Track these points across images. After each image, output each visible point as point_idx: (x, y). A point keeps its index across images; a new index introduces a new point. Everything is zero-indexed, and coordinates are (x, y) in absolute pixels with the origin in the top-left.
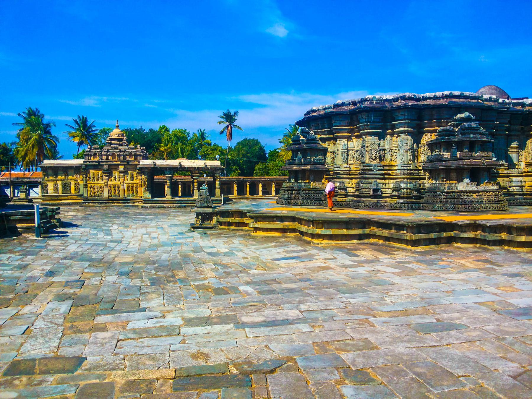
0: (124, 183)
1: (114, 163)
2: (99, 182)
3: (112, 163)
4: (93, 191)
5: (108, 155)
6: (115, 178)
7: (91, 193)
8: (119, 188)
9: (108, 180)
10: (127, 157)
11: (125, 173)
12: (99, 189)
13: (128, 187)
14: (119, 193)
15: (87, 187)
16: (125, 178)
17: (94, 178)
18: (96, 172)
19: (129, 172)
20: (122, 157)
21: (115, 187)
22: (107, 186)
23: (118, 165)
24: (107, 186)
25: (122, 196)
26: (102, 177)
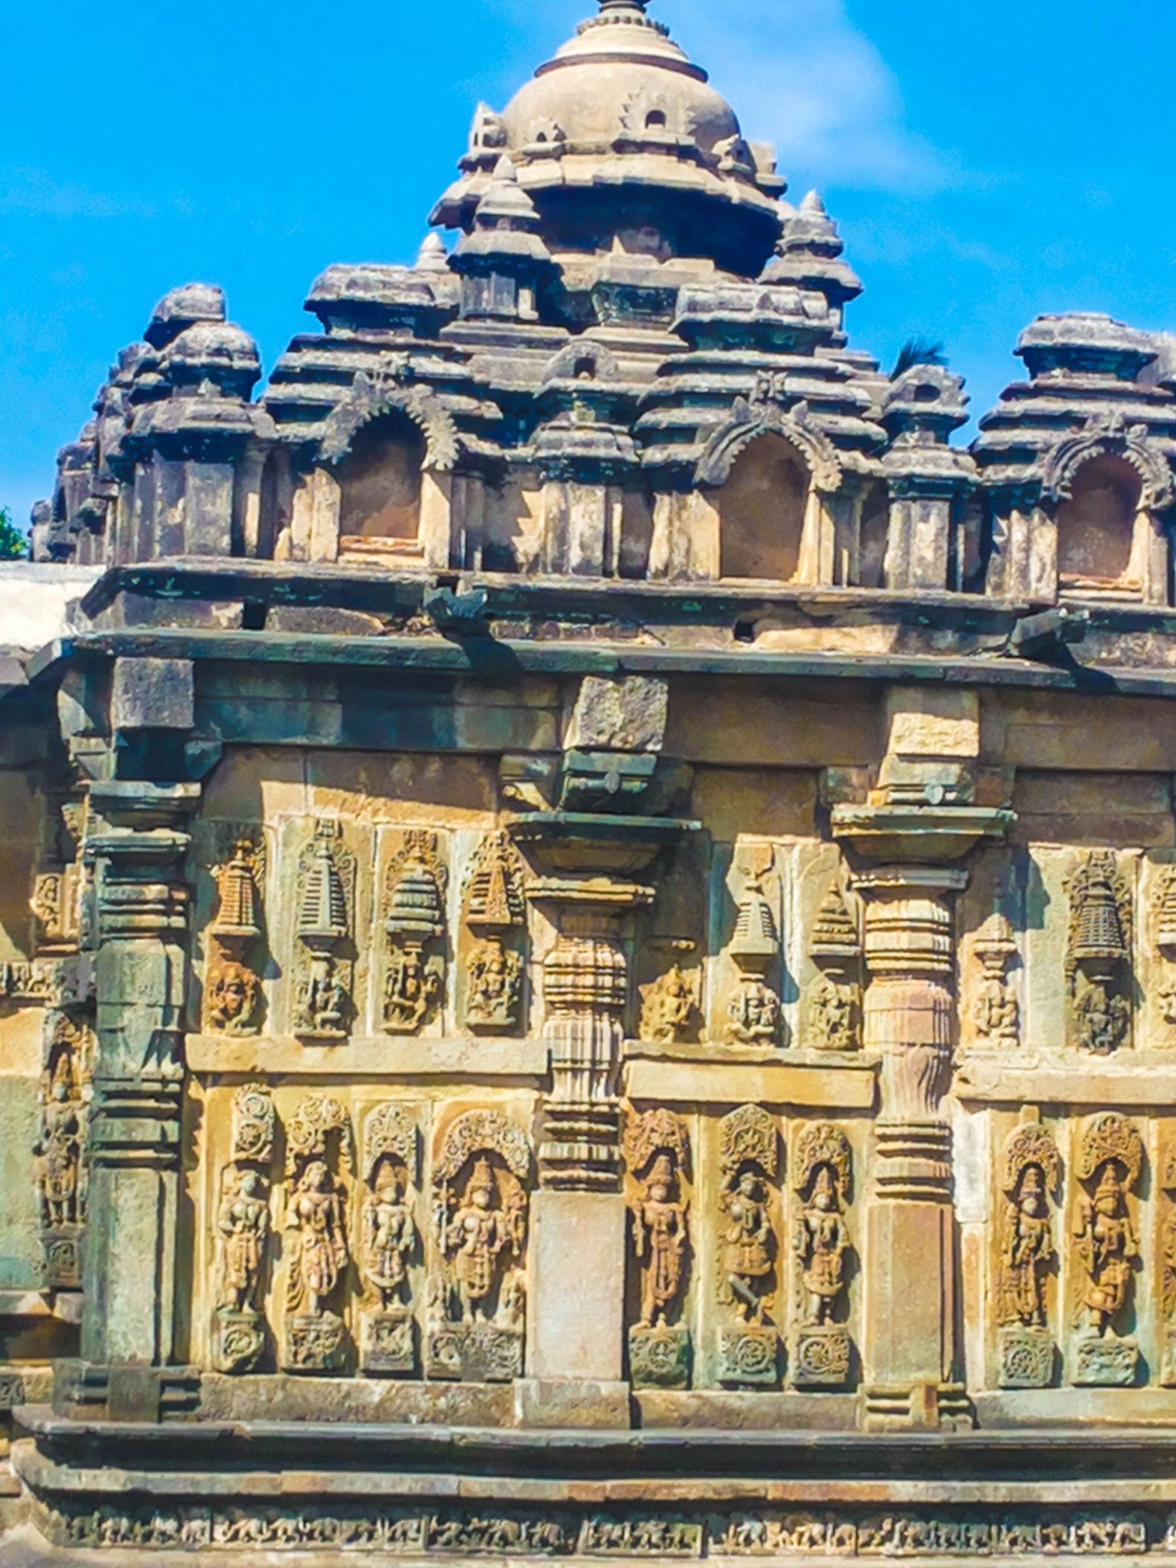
0: (938, 1078)
1: (775, 644)
2: (445, 1042)
3: (712, 644)
4: (304, 1258)
5: (641, 485)
6: (768, 968)
7: (253, 1289)
8: (835, 1176)
9: (624, 1009)
10: (1029, 542)
11: (978, 870)
12: (424, 1206)
13: (1031, 1181)
14: (836, 1306)
15: (177, 1157)
16: (975, 986)
17: (339, 948)
18: (379, 822)
19: (1055, 861)
20: (918, 545)
21: (754, 1173)
22: (595, 1148)
23: (859, 701)
24: (595, 1148)
25: (895, 1389)
26: (511, 935)
